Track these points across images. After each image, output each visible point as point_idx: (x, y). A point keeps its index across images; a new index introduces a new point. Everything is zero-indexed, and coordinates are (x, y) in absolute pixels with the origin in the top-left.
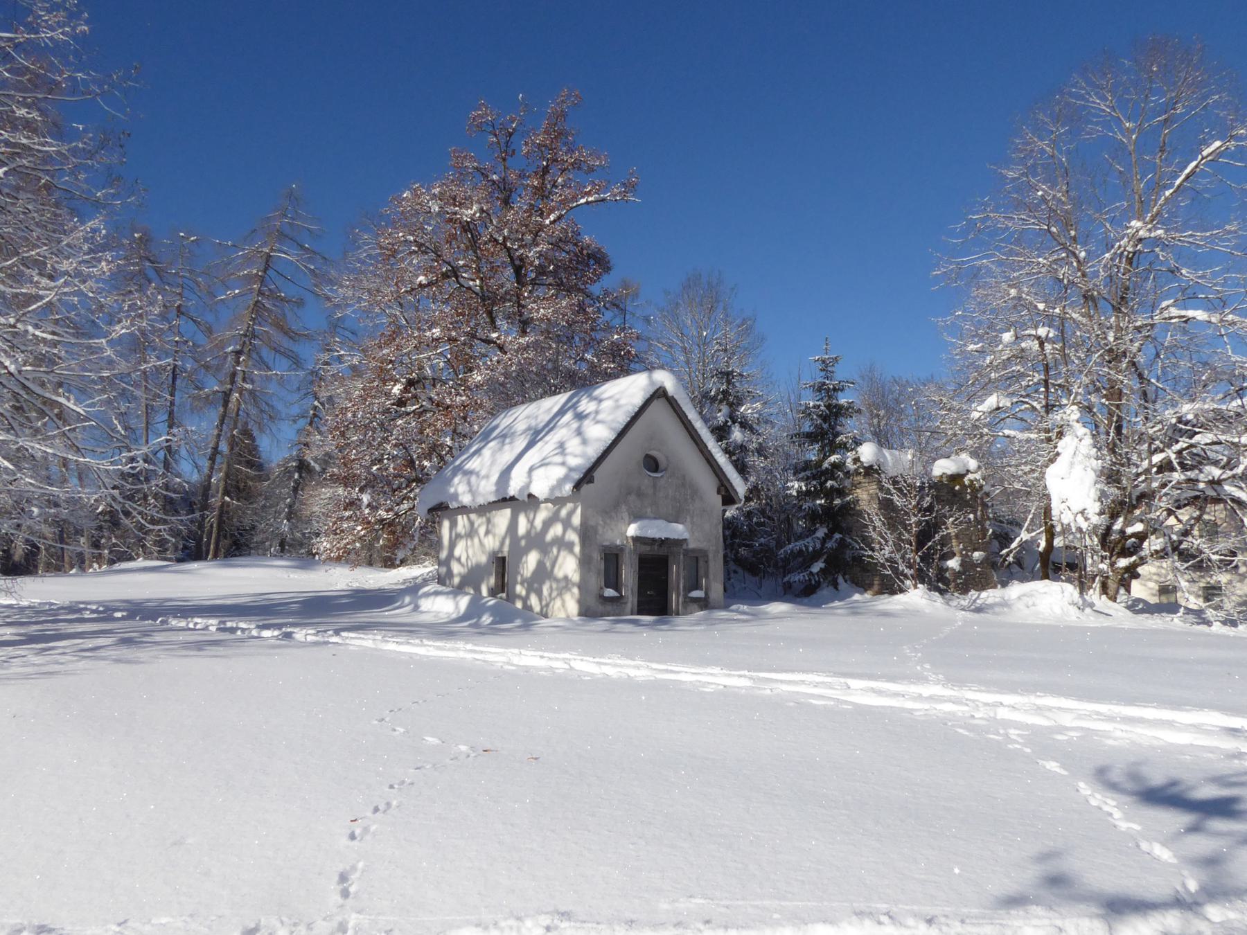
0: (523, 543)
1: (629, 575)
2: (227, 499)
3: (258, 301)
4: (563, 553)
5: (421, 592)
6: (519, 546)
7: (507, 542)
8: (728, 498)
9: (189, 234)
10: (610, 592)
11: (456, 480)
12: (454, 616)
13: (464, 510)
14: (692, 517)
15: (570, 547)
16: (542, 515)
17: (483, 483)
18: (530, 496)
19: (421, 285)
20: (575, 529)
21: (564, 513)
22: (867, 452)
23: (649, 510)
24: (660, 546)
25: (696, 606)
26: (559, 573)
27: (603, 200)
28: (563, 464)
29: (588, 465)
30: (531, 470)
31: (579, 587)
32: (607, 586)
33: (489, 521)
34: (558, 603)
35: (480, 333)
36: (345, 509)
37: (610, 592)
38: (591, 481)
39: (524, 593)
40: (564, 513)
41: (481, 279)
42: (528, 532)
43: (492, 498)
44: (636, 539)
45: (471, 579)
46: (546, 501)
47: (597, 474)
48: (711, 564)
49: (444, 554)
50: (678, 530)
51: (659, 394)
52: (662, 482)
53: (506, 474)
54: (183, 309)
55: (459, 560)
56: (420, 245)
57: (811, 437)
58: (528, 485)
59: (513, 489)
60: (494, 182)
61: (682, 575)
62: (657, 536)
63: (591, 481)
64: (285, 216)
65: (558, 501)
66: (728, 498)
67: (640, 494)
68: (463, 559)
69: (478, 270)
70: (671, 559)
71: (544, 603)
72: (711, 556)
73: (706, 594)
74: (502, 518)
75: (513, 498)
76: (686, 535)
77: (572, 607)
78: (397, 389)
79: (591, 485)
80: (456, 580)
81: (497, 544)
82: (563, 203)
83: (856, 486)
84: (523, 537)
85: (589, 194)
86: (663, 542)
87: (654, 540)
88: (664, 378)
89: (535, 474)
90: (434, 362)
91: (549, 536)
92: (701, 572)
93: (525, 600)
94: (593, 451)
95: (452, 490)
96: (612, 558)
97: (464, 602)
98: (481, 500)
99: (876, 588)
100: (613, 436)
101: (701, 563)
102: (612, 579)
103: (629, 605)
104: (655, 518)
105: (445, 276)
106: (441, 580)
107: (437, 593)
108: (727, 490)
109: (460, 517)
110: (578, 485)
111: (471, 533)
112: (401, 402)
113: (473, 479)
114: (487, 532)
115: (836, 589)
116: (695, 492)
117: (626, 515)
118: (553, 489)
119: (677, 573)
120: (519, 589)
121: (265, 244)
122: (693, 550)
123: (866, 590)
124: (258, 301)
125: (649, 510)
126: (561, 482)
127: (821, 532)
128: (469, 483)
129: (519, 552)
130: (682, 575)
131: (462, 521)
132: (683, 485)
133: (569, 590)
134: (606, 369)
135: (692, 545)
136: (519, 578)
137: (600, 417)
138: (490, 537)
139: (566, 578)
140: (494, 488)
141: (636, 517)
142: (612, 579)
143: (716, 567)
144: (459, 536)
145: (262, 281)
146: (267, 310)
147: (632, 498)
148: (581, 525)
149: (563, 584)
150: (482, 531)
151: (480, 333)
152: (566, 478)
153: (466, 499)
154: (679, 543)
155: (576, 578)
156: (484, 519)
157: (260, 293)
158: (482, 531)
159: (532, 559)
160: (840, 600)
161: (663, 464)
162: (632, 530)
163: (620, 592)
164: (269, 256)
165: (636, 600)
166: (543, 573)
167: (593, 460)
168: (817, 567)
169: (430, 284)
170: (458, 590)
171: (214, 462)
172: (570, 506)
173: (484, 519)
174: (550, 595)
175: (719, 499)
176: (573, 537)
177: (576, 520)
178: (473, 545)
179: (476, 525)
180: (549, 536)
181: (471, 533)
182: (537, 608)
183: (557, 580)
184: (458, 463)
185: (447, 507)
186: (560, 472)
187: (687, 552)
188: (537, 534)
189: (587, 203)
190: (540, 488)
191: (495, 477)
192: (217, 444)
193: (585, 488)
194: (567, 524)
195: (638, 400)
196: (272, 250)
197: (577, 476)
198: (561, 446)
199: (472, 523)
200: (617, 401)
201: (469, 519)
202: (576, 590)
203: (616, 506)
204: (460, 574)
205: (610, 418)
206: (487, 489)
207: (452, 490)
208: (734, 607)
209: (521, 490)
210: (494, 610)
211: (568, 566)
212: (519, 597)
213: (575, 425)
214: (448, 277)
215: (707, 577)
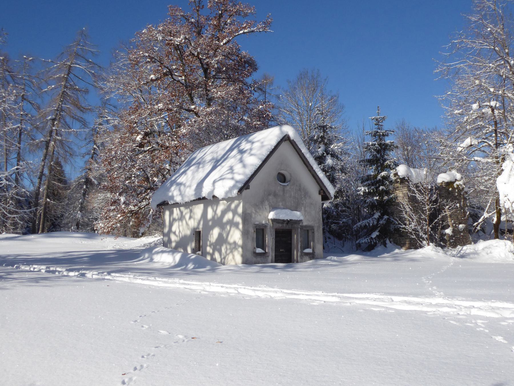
0: (210, 223)
1: (270, 240)
2: (48, 200)
3: (64, 91)
4: (233, 229)
5: (154, 251)
6: (208, 225)
7: (202, 223)
8: (325, 197)
9: (29, 56)
10: (259, 250)
11: (173, 188)
12: (173, 264)
13: (177, 205)
14: (305, 208)
15: (236, 225)
16: (221, 207)
17: (188, 190)
18: (214, 197)
19: (152, 80)
20: (239, 215)
21: (233, 206)
22: (402, 170)
23: (281, 204)
24: (287, 224)
25: (307, 257)
26: (231, 240)
27: (253, 31)
28: (232, 179)
29: (246, 179)
30: (214, 182)
31: (242, 248)
32: (258, 247)
33: (191, 211)
34: (230, 257)
35: (185, 106)
36: (111, 205)
38: (248, 188)
39: (211, 251)
40: (233, 206)
41: (185, 76)
42: (213, 217)
43: (193, 198)
44: (273, 220)
45: (182, 244)
46: (223, 199)
47: (251, 184)
48: (316, 234)
49: (166, 230)
50: (297, 215)
51: (286, 138)
52: (288, 188)
53: (200, 185)
54: (25, 97)
55: (175, 233)
57: (371, 162)
58: (213, 191)
59: (205, 193)
60: (192, 23)
61: (299, 240)
62: (285, 219)
63: (248, 188)
64: (79, 45)
65: (229, 199)
66: (325, 197)
67: (275, 195)
68: (177, 233)
69: (184, 71)
70: (293, 231)
71: (223, 257)
72: (316, 229)
73: (313, 250)
74: (199, 209)
75: (204, 198)
76: (302, 218)
77: (238, 259)
78: (139, 138)
79: (248, 190)
80: (174, 244)
81: (196, 224)
82: (230, 33)
83: (396, 189)
84: (210, 220)
85: (245, 28)
86: (289, 222)
87: (283, 221)
88: (289, 130)
89: (217, 184)
90: (159, 122)
91: (225, 220)
92: (310, 238)
93: (212, 255)
94: (249, 171)
95: (170, 194)
96: (260, 231)
97: (178, 256)
98: (187, 200)
99: (407, 246)
100: (259, 163)
101: (310, 233)
102: (261, 243)
104: (284, 208)
105: (165, 74)
106: (165, 245)
107: (163, 252)
108: (324, 192)
109: (175, 209)
110: (240, 191)
111: (182, 218)
112: (141, 145)
113: (182, 188)
114: (190, 217)
115: (386, 247)
116: (306, 194)
118: (227, 193)
119: (296, 239)
120: (209, 249)
121: (68, 60)
122: (306, 226)
123: (402, 247)
125: (281, 204)
126: (231, 189)
127: (377, 215)
128: (180, 190)
129: (208, 228)
130: (299, 240)
131: (176, 212)
132: (300, 190)
133: (237, 249)
134: (255, 125)
135: (305, 224)
136: (208, 243)
137: (253, 152)
138: (192, 220)
139: (235, 243)
140: (193, 193)
142: (261, 243)
143: (319, 235)
144: (174, 220)
145: (67, 80)
146: (69, 96)
147: (271, 197)
148: (243, 213)
150: (187, 217)
151: (185, 106)
152: (234, 187)
153: (178, 199)
154: (298, 222)
155: (240, 242)
156: (188, 210)
157: (65, 87)
158: (187, 217)
159: (215, 232)
160: (387, 253)
161: (288, 177)
162: (271, 215)
163: (265, 251)
164: (70, 67)
165: (274, 254)
166: (222, 240)
167: (249, 176)
168: (375, 234)
169: (157, 79)
170: (175, 250)
171: (41, 180)
172: (236, 202)
173: (188, 210)
174: (226, 252)
175: (320, 197)
176: (238, 219)
177: (240, 210)
178: (182, 225)
179: (184, 213)
180: (225, 220)
181: (182, 218)
182: (219, 260)
183: (230, 244)
184: (173, 178)
185: (168, 204)
186: (231, 183)
187: (302, 227)
188: (218, 218)
189: (244, 33)
190: (220, 193)
191: (194, 187)
192: (43, 169)
193: (245, 192)
194: (235, 212)
195: (274, 143)
196: (72, 63)
197: (240, 185)
198: (231, 169)
199: (182, 213)
200: (262, 143)
201: (180, 210)
202: (240, 249)
203: (262, 202)
204: (175, 241)
205: (259, 152)
206: (190, 194)
207: (170, 194)
208: (329, 258)
209: (209, 193)
210: (194, 261)
211: (236, 236)
212: (209, 253)
213: (239, 157)
214: (167, 75)
215: (314, 241)
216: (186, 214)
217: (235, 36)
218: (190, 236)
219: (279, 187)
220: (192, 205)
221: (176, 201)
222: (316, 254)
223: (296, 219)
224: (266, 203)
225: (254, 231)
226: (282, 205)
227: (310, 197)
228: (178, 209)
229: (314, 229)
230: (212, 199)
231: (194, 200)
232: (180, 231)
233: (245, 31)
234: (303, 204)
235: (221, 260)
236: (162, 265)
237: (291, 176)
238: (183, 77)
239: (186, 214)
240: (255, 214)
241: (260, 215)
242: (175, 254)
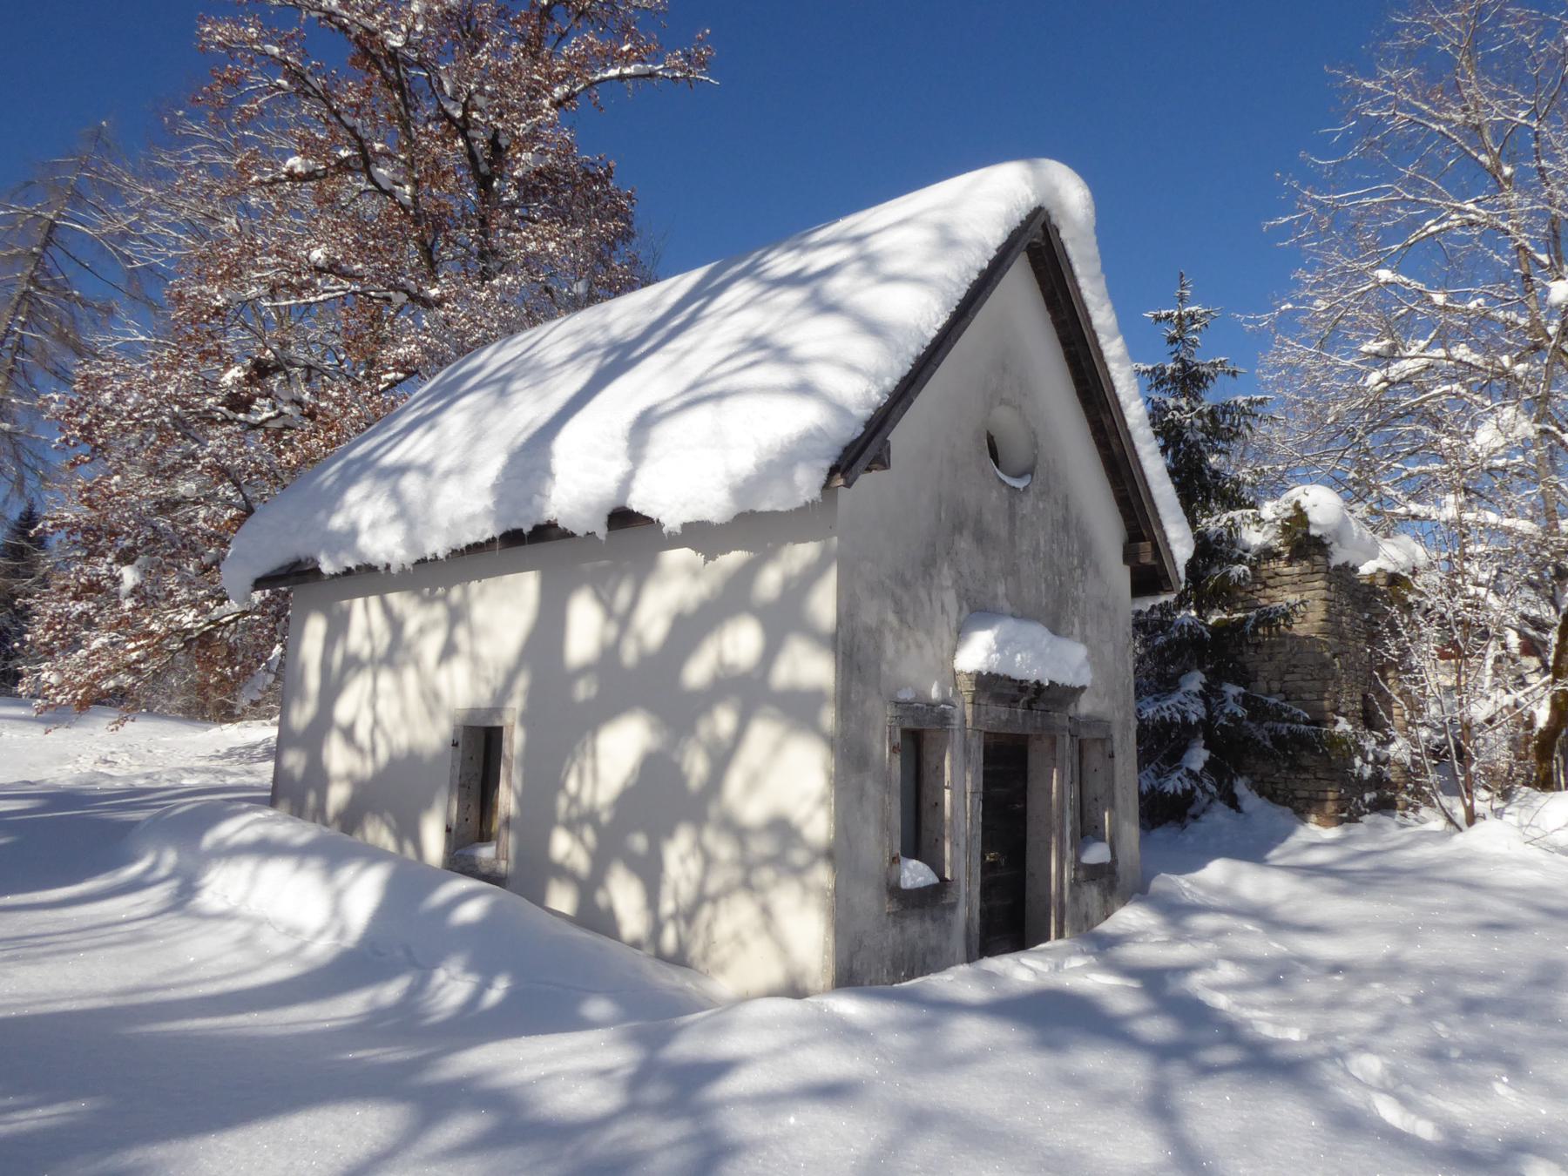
5: (208, 840)
7: (522, 683)
10: (915, 874)
11: (354, 494)
12: (322, 949)
13: (367, 577)
14: (1083, 623)
16: (677, 582)
19: (291, 175)
21: (770, 580)
22: (1322, 504)
27: (652, 75)
30: (645, 423)
33: (457, 616)
36: (77, 598)
37: (915, 874)
40: (770, 580)
42: (609, 653)
43: (487, 530)
44: (989, 685)
45: (390, 793)
47: (900, 438)
49: (301, 715)
55: (348, 734)
56: (296, 76)
58: (626, 482)
64: (85, 168)
66: (1148, 578)
67: (981, 537)
68: (362, 733)
69: (411, 164)
71: (668, 906)
74: (506, 608)
75: (547, 532)
76: (1085, 678)
77: (807, 931)
78: (235, 373)
80: (338, 795)
84: (585, 670)
85: (626, 59)
87: (1021, 686)
89: (666, 435)
90: (316, 340)
91: (698, 672)
93: (589, 887)
95: (338, 522)
96: (918, 740)
97: (364, 891)
98: (437, 546)
99: (1330, 807)
101: (1094, 758)
103: (962, 912)
105: (343, 166)
106: (291, 794)
107: (265, 849)
112: (239, 403)
113: (411, 485)
114: (448, 651)
117: (950, 598)
119: (1054, 786)
121: (48, 208)
124: (27, 292)
127: (1195, 681)
129: (567, 722)
135: (1085, 706)
136: (562, 803)
140: (488, 501)
141: (978, 612)
144: (353, 663)
149: (762, 846)
153: (384, 543)
155: (818, 827)
156: (439, 611)
157: (33, 280)
158: (431, 646)
159: (621, 748)
162: (977, 653)
163: (940, 873)
164: (52, 225)
165: (977, 890)
169: (310, 176)
170: (336, 848)
172: (802, 553)
173: (439, 611)
175: (1121, 577)
176: (809, 667)
177: (824, 604)
178: (400, 690)
179: (411, 628)
180: (698, 672)
181: (396, 654)
183: (737, 831)
185: (317, 572)
188: (645, 659)
189: (621, 77)
191: (491, 466)
193: (867, 482)
194: (783, 621)
196: (59, 216)
199: (396, 624)
201: (387, 610)
202: (823, 875)
203: (928, 566)
204: (349, 776)
206: (464, 506)
207: (338, 522)
211: (788, 778)
212: (562, 872)
214: (349, 170)
216: (422, 631)
217: (592, 84)
218: (438, 758)
219: (995, 494)
220: (465, 579)
221: (360, 555)
222: (1120, 868)
223: (1068, 683)
224: (946, 575)
225: (894, 749)
226: (1006, 595)
227: (1097, 572)
228: (374, 601)
229: (1110, 738)
230: (602, 532)
231: (475, 548)
232: (376, 722)
233: (627, 71)
234: (1075, 601)
235: (657, 929)
236: (246, 942)
237: (1035, 445)
238: (408, 189)
239: (422, 631)
240: (899, 638)
241: (920, 646)
242: (347, 873)
